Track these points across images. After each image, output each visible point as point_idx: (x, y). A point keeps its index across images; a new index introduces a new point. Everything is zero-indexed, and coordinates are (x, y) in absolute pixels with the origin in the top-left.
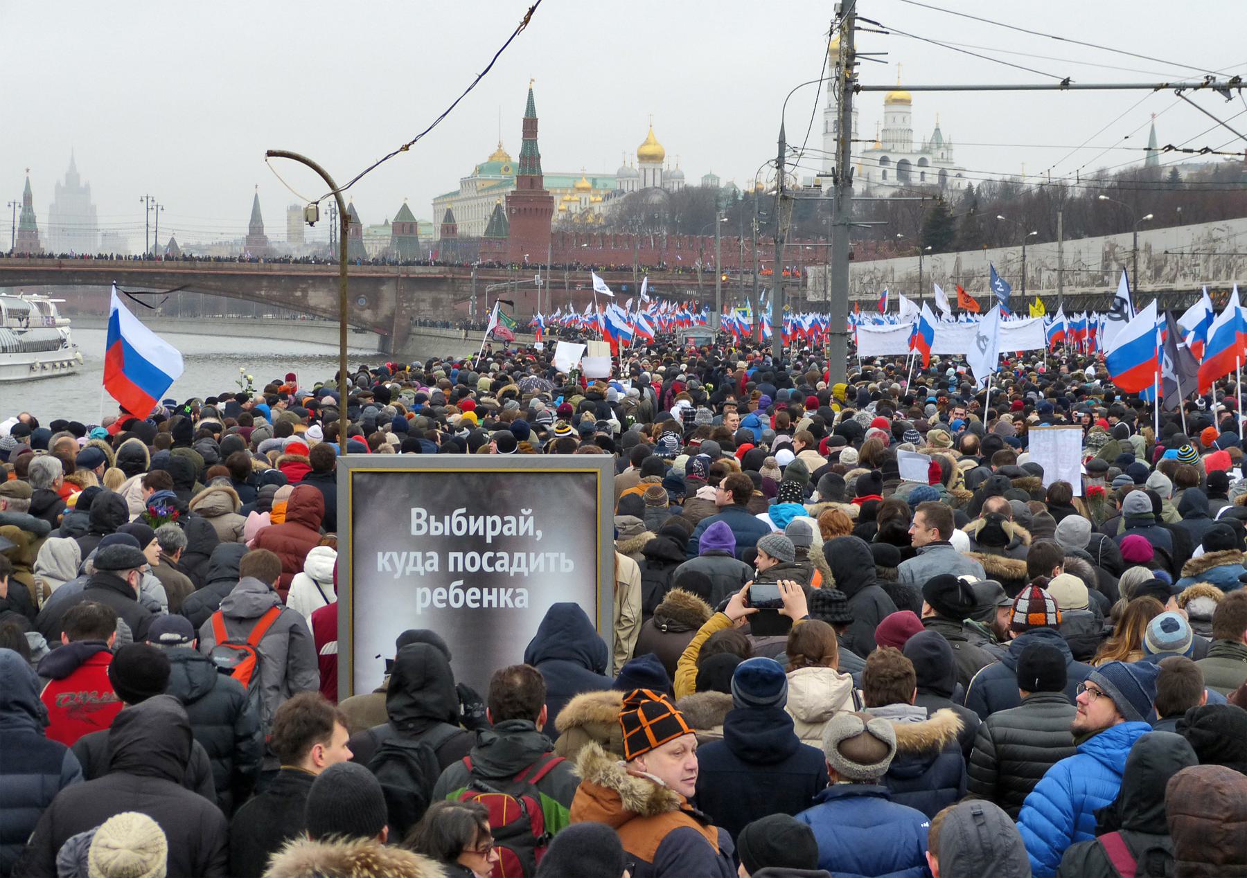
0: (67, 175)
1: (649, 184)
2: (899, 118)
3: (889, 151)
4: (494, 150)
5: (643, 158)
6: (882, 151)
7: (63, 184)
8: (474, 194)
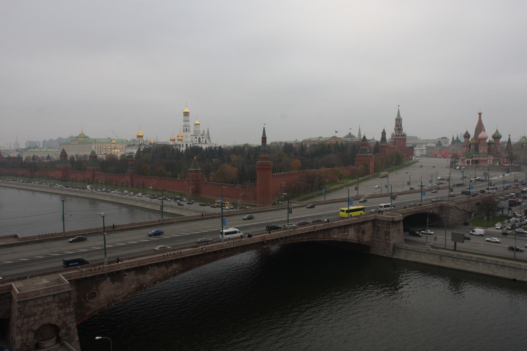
1: (141, 143)
2: (198, 128)
3: (197, 135)
4: (80, 133)
6: (195, 135)
8: (78, 143)
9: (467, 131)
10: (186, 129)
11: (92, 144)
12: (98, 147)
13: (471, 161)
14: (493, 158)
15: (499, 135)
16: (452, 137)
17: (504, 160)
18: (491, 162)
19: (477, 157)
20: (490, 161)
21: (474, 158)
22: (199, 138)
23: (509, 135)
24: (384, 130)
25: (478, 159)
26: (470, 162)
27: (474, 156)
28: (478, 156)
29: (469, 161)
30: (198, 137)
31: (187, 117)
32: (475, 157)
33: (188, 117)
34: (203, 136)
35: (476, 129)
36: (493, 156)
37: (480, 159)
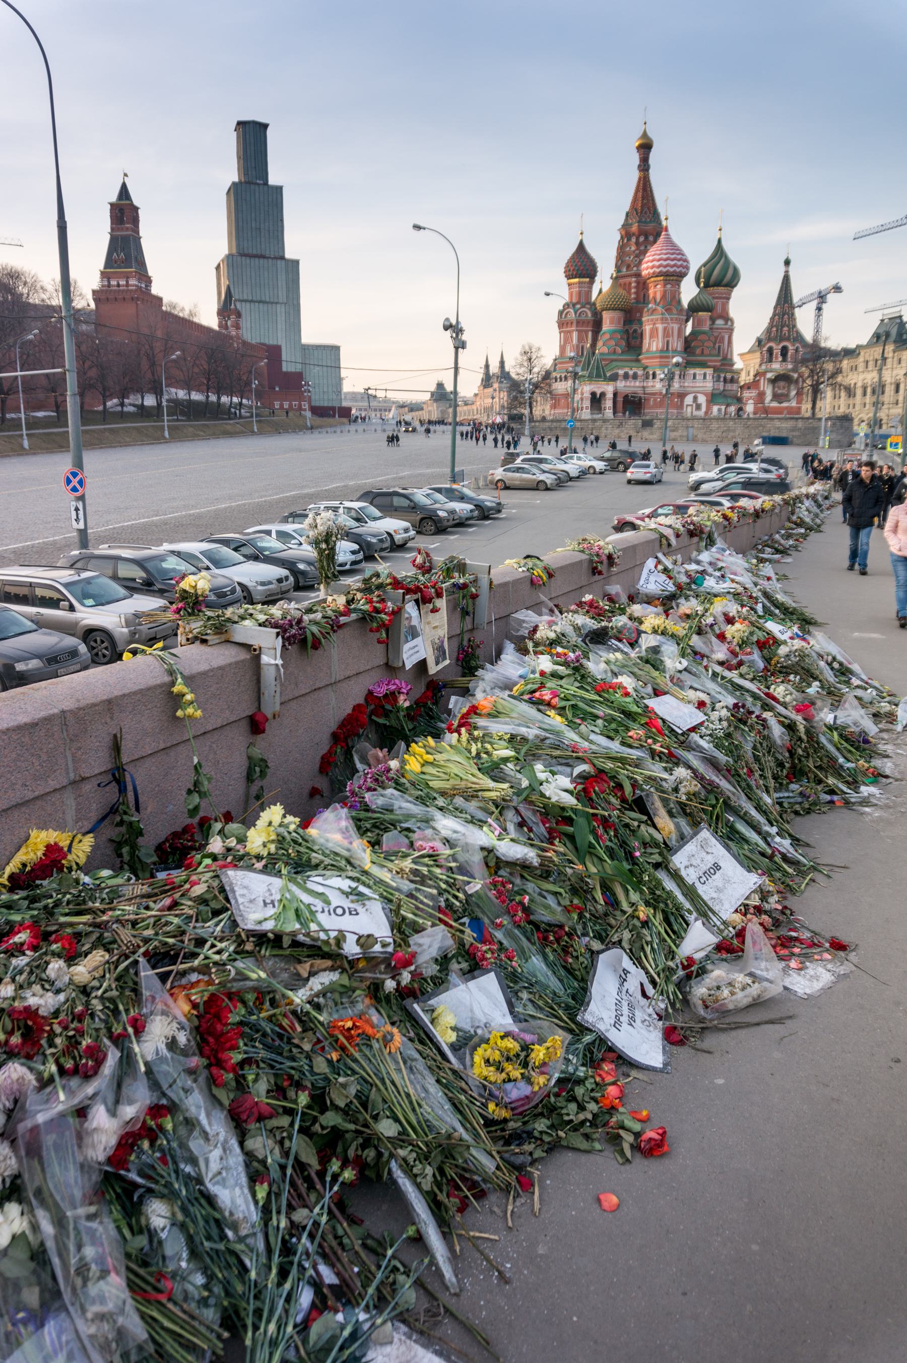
9: (581, 247)
13: (610, 395)
14: (709, 385)
15: (730, 272)
16: (484, 363)
17: (762, 395)
18: (698, 407)
19: (635, 376)
20: (695, 398)
21: (621, 384)
23: (787, 263)
24: (124, 192)
25: (640, 391)
26: (608, 403)
27: (621, 372)
28: (640, 372)
29: (603, 394)
32: (626, 376)
35: (626, 234)
36: (709, 371)
37: (649, 390)
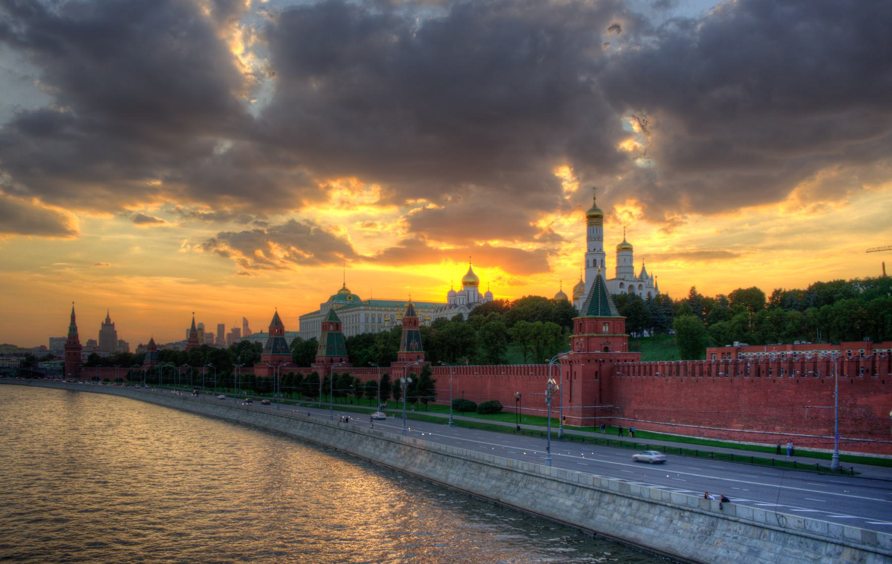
0: (106, 319)
3: (623, 279)
4: (341, 287)
5: (465, 284)
7: (104, 323)
10: (595, 261)
11: (360, 310)
12: (373, 319)
22: (631, 287)
30: (627, 284)
31: (595, 228)
33: (598, 228)
34: (642, 281)
